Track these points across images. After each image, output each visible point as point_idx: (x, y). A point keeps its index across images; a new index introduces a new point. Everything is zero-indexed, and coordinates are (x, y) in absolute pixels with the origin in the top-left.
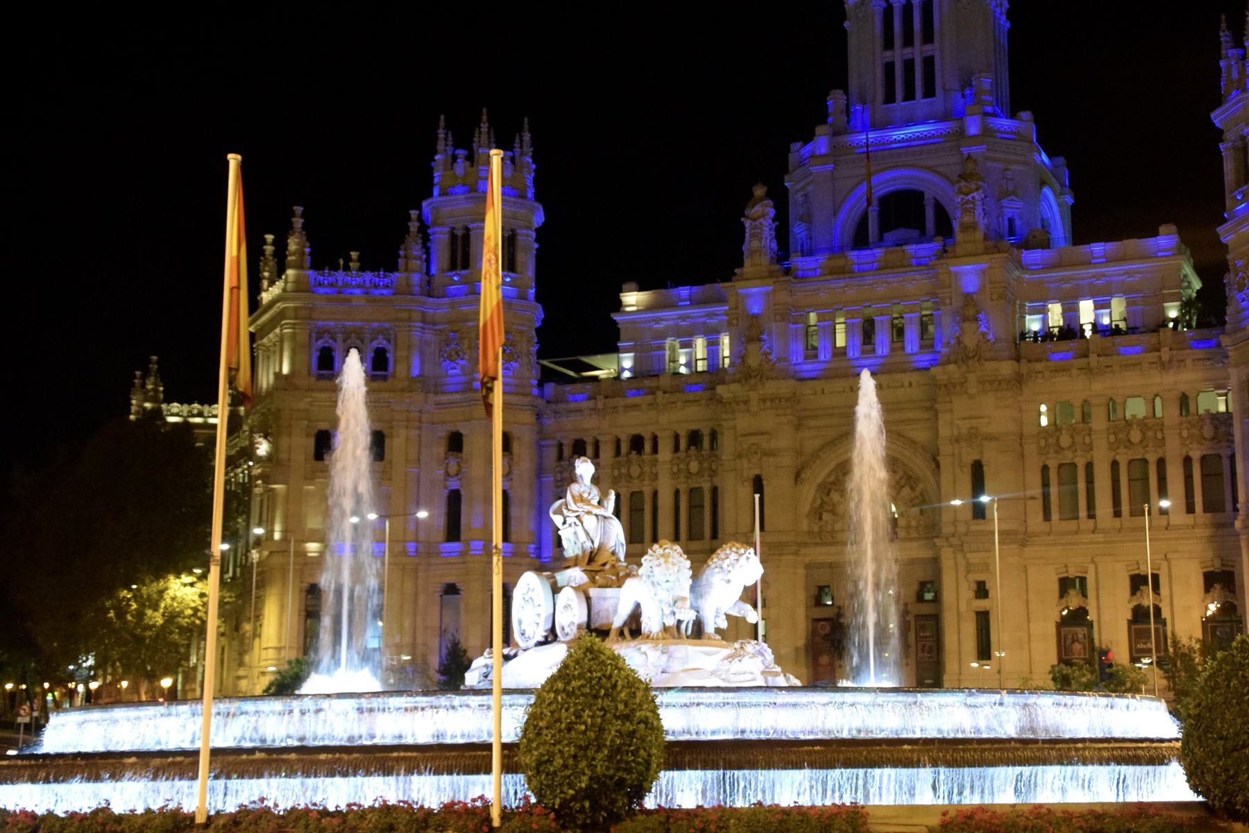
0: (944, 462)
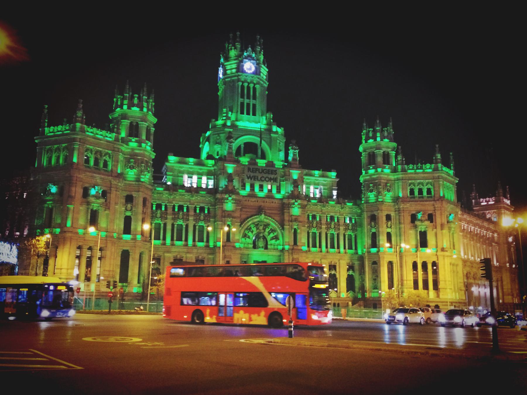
0: (286, 227)
